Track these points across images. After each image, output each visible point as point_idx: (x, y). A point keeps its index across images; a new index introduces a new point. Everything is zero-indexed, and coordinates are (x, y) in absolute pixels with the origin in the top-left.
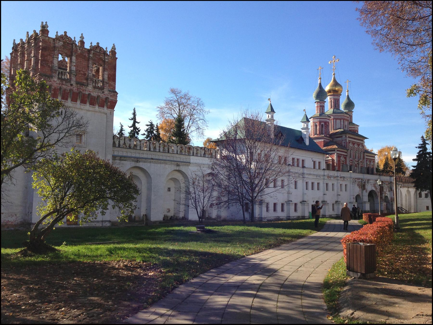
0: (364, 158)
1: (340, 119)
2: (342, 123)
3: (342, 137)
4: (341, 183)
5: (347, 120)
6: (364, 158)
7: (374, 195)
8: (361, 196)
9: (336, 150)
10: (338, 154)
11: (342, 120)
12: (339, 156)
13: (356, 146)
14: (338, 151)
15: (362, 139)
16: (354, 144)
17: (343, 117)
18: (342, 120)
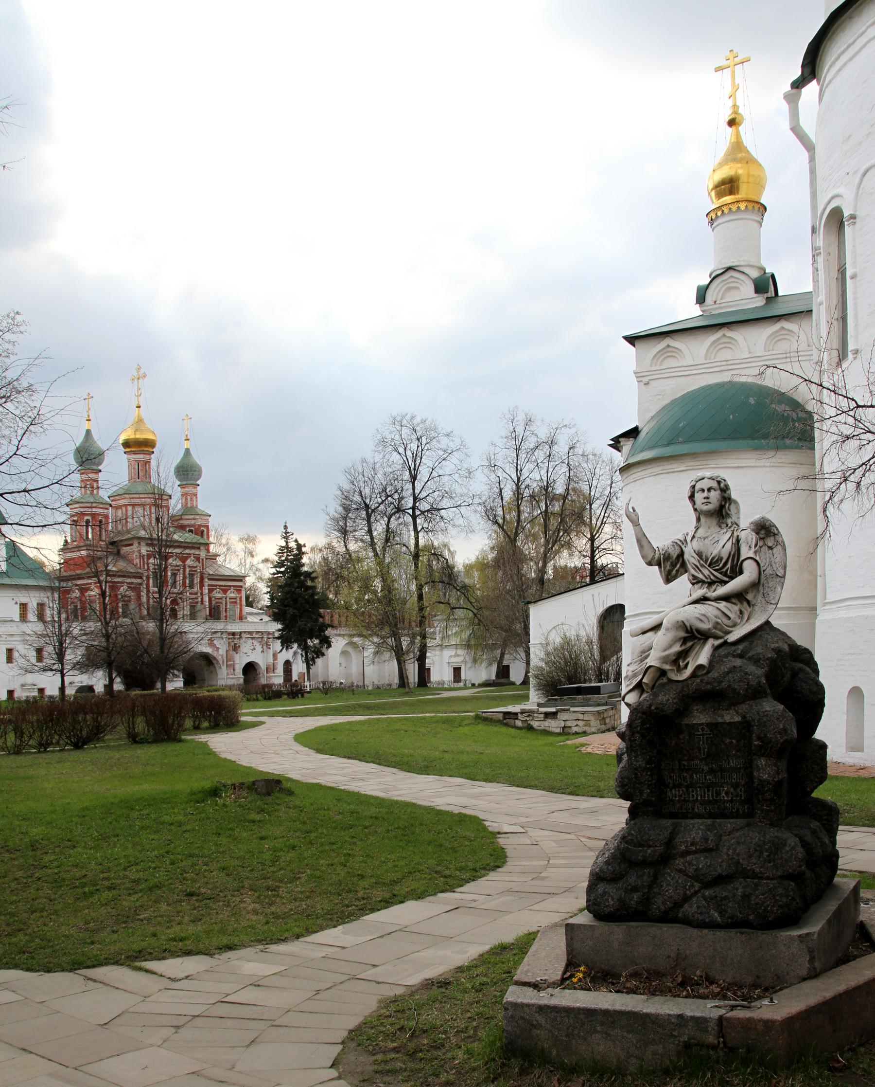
7: (214, 662)
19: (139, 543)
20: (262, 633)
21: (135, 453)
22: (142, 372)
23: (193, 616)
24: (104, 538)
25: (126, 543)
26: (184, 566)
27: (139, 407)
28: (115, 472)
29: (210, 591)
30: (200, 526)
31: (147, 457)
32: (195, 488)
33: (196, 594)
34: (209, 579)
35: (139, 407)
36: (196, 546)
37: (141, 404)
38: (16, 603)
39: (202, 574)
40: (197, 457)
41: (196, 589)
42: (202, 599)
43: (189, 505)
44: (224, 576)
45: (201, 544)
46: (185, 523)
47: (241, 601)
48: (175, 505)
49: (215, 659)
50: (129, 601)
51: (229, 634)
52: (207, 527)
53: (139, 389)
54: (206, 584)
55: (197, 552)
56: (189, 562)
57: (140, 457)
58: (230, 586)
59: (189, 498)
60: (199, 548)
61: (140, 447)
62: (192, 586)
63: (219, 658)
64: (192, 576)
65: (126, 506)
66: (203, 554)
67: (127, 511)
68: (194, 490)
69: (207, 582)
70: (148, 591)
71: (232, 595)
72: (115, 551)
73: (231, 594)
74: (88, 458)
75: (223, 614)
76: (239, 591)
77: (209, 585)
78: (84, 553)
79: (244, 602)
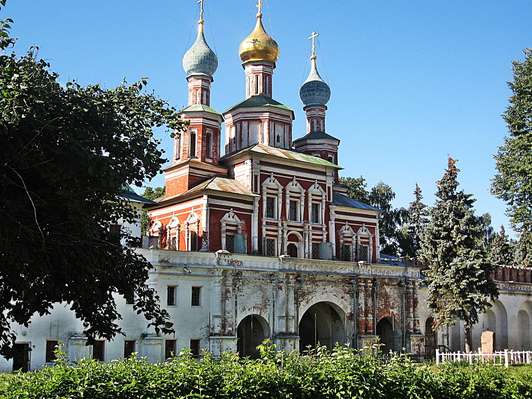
0: (328, 219)
5: (284, 124)
6: (328, 219)
13: (294, 187)
15: (324, 170)
16: (284, 181)
29: (338, 227)
30: (327, 152)
39: (328, 204)
42: (328, 235)
43: (315, 129)
47: (374, 241)
52: (336, 154)
55: (322, 178)
56: (313, 190)
59: (315, 121)
67: (241, 127)
68: (321, 113)
69: (334, 216)
73: (363, 232)
76: (372, 230)
77: (336, 220)
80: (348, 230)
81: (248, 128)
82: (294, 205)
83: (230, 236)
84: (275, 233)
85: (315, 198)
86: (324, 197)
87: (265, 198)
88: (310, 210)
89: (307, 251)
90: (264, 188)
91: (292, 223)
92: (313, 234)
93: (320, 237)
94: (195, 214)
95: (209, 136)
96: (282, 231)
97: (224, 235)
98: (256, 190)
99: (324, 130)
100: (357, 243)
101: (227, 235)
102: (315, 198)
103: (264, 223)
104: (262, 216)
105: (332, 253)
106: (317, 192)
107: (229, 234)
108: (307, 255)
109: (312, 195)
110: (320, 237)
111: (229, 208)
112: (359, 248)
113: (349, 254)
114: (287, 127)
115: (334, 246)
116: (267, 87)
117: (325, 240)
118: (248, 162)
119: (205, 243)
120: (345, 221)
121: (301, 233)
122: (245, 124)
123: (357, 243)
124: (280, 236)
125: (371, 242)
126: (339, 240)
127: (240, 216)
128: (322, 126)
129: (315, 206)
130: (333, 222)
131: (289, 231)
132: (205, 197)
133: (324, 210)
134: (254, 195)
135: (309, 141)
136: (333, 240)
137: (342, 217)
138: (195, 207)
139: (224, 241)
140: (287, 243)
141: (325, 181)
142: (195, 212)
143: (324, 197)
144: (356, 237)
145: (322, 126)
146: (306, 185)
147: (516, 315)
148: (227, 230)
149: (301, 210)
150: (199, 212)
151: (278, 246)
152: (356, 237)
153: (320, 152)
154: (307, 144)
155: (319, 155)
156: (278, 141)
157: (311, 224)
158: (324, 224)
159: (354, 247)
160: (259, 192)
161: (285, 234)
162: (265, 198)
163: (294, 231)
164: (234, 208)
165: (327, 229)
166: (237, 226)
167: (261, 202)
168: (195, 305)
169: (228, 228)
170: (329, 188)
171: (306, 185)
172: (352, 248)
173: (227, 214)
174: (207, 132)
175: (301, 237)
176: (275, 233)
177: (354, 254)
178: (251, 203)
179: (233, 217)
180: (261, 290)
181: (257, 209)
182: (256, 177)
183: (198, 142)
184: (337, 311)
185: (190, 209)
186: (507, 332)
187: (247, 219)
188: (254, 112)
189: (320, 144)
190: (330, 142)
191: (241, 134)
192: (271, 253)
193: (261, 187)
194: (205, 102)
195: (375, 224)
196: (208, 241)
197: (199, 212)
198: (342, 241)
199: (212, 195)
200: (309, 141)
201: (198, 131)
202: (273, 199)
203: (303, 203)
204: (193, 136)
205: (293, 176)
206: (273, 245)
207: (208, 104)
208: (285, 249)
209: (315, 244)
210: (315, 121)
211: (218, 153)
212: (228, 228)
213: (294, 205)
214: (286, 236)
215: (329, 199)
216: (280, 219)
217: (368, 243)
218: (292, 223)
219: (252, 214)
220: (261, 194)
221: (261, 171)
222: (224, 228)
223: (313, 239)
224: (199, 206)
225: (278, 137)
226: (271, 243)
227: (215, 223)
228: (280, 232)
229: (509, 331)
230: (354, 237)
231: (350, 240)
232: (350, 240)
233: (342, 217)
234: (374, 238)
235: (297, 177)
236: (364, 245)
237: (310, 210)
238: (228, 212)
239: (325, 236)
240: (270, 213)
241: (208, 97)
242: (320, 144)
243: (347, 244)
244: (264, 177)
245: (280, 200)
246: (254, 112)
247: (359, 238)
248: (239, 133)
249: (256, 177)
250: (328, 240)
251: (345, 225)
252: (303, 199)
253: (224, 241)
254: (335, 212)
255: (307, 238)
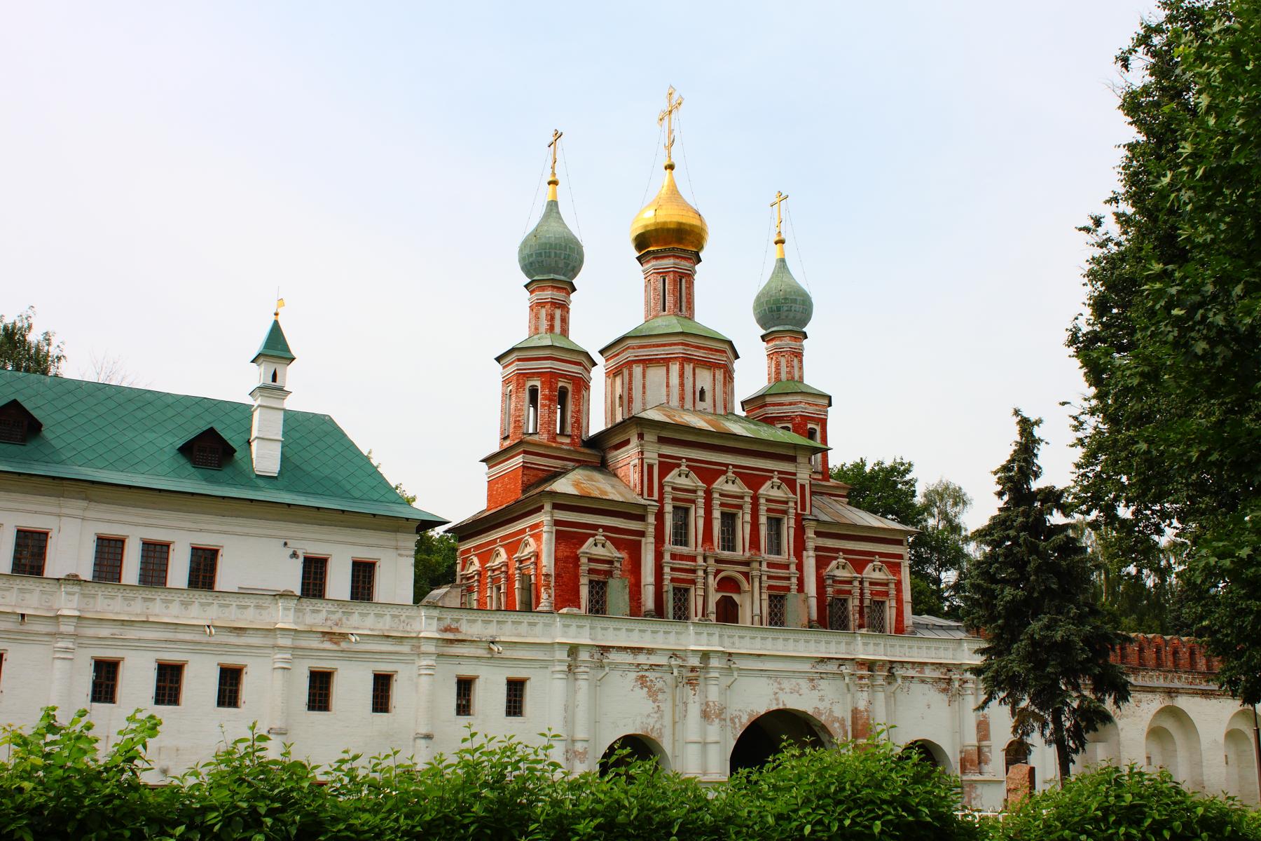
0: (800, 547)
1: (666, 362)
2: (675, 380)
3: (627, 442)
4: (466, 671)
5: (711, 366)
6: (800, 547)
8: (666, 745)
9: (548, 507)
10: (557, 523)
11: (675, 368)
12: (568, 538)
14: (556, 506)
15: (791, 453)
16: (708, 474)
17: (678, 349)
18: (675, 368)
19: (641, 436)
20: (949, 668)
21: (657, 256)
22: (675, 96)
23: (777, 617)
24: (569, 430)
25: (617, 440)
26: (755, 499)
27: (671, 167)
28: (613, 299)
29: (821, 563)
31: (685, 264)
32: (800, 340)
33: (787, 567)
34: (818, 534)
35: (671, 167)
36: (788, 454)
37: (675, 160)
38: (294, 555)
39: (800, 520)
40: (804, 277)
41: (787, 555)
42: (801, 582)
43: (784, 376)
44: (855, 526)
45: (795, 447)
46: (772, 411)
48: (752, 374)
49: (823, 727)
50: (609, 574)
51: (862, 663)
52: (823, 423)
53: (671, 132)
54: (810, 544)
56: (765, 490)
57: (668, 263)
58: (872, 554)
59: (783, 361)
60: (793, 459)
61: (671, 247)
62: (776, 548)
63: (835, 728)
64: (775, 524)
65: (630, 364)
66: (803, 476)
67: (631, 375)
68: (794, 344)
69: (812, 541)
70: (659, 556)
71: (877, 575)
72: (597, 460)
73: (870, 573)
74: (552, 267)
75: (854, 618)
76: (895, 568)
77: (817, 549)
78: (518, 460)
79: (907, 596)
80: (844, 567)
81: (644, 377)
82: (729, 520)
83: (598, 582)
84: (691, 576)
85: (773, 506)
86: (791, 504)
87: (668, 508)
88: (763, 531)
89: (757, 611)
90: (668, 489)
91: (727, 554)
92: (769, 577)
93: (785, 583)
94: (531, 540)
95: (563, 394)
96: (705, 571)
97: (584, 581)
98: (651, 493)
99: (801, 378)
100: (862, 594)
101: (591, 582)
102: (773, 506)
103: (667, 557)
104: (664, 542)
105: (809, 613)
106: (776, 494)
107: (595, 577)
108: (756, 618)
109: (768, 500)
110: (785, 583)
111: (596, 527)
112: (867, 603)
113: (847, 617)
114: (720, 375)
115: (813, 602)
116: (684, 299)
117: (794, 587)
118: (634, 441)
119: (544, 596)
120: (837, 550)
121: (746, 575)
122: (637, 370)
123: (862, 594)
124: (700, 581)
125: (893, 592)
126: (825, 587)
127: (618, 544)
128: (796, 369)
129: (774, 523)
130: (812, 553)
131: (718, 572)
132: (548, 507)
133: (792, 531)
134: (644, 502)
135: (768, 400)
136: (811, 587)
137: (830, 543)
138: (533, 527)
139: (584, 592)
140: (714, 598)
141: (795, 474)
142: (531, 536)
143: (791, 504)
144: (861, 582)
145: (796, 369)
146: (754, 480)
147: (1221, 739)
148: (591, 571)
149: (743, 531)
150: (537, 537)
151: (695, 600)
152: (861, 582)
153: (791, 419)
154: (765, 405)
155: (790, 425)
156: (702, 399)
157: (765, 556)
158: (793, 559)
159: (857, 602)
160: (656, 496)
161: (711, 578)
162: (668, 508)
163: (730, 571)
164: (606, 528)
165: (800, 567)
166: (610, 562)
167: (660, 516)
168: (382, 711)
169: (593, 565)
170: (803, 486)
171: (754, 480)
172: (853, 604)
173: (591, 540)
174: (560, 384)
175: (745, 585)
176: (691, 576)
177: (857, 616)
178: (642, 518)
179: (603, 546)
180: (643, 685)
181: (651, 530)
182: (650, 467)
183: (543, 405)
184: (816, 729)
185: (523, 531)
186: (1201, 774)
187: (634, 550)
188: (654, 346)
189: (791, 404)
190: (811, 400)
191: (630, 389)
192: (682, 614)
193: (661, 487)
194: (558, 329)
195: (900, 557)
196: (552, 591)
197: (537, 537)
198: (830, 590)
199: (562, 503)
200: (768, 400)
201: (543, 383)
202: (687, 510)
203: (748, 518)
204: (533, 392)
205: (727, 465)
206: (687, 600)
207: (565, 332)
208: (712, 607)
209: (776, 597)
210: (783, 361)
211: (584, 424)
212: (593, 565)
213: (729, 520)
214: (712, 582)
215: (803, 508)
216: (700, 550)
217: (886, 594)
218: (727, 554)
219: (643, 540)
220: (661, 499)
221: (660, 456)
222: (584, 565)
223: (770, 587)
224: (536, 526)
225: (702, 392)
226: (682, 594)
227: (567, 557)
228: (701, 573)
229: (1205, 771)
230: (856, 583)
231: (847, 587)
232: (847, 587)
233: (830, 543)
234: (899, 584)
235: (735, 466)
236: (877, 598)
237: (763, 531)
238: (593, 536)
239: (794, 580)
240: (681, 536)
241: (564, 320)
242: (791, 404)
243: (842, 596)
244: (665, 468)
245: (701, 512)
246: (654, 346)
247: (866, 584)
248: (626, 386)
249: (650, 467)
250: (801, 588)
251: (836, 558)
252: (748, 508)
253: (584, 592)
254: (816, 533)
255: (757, 584)
